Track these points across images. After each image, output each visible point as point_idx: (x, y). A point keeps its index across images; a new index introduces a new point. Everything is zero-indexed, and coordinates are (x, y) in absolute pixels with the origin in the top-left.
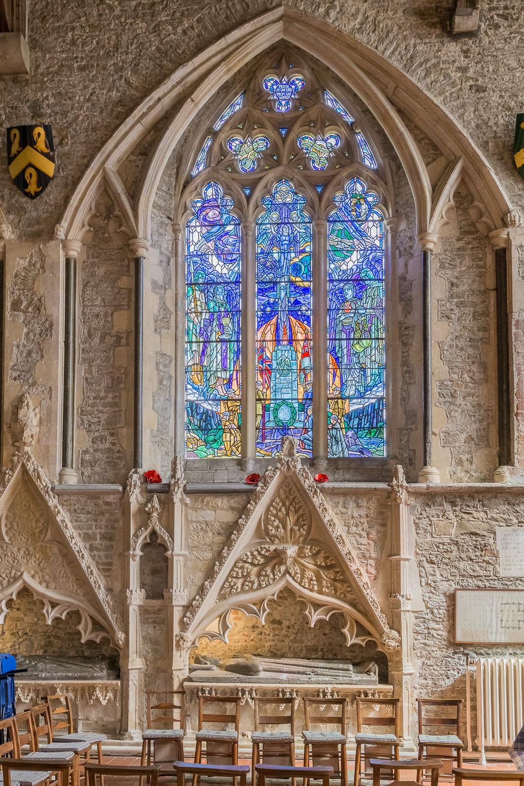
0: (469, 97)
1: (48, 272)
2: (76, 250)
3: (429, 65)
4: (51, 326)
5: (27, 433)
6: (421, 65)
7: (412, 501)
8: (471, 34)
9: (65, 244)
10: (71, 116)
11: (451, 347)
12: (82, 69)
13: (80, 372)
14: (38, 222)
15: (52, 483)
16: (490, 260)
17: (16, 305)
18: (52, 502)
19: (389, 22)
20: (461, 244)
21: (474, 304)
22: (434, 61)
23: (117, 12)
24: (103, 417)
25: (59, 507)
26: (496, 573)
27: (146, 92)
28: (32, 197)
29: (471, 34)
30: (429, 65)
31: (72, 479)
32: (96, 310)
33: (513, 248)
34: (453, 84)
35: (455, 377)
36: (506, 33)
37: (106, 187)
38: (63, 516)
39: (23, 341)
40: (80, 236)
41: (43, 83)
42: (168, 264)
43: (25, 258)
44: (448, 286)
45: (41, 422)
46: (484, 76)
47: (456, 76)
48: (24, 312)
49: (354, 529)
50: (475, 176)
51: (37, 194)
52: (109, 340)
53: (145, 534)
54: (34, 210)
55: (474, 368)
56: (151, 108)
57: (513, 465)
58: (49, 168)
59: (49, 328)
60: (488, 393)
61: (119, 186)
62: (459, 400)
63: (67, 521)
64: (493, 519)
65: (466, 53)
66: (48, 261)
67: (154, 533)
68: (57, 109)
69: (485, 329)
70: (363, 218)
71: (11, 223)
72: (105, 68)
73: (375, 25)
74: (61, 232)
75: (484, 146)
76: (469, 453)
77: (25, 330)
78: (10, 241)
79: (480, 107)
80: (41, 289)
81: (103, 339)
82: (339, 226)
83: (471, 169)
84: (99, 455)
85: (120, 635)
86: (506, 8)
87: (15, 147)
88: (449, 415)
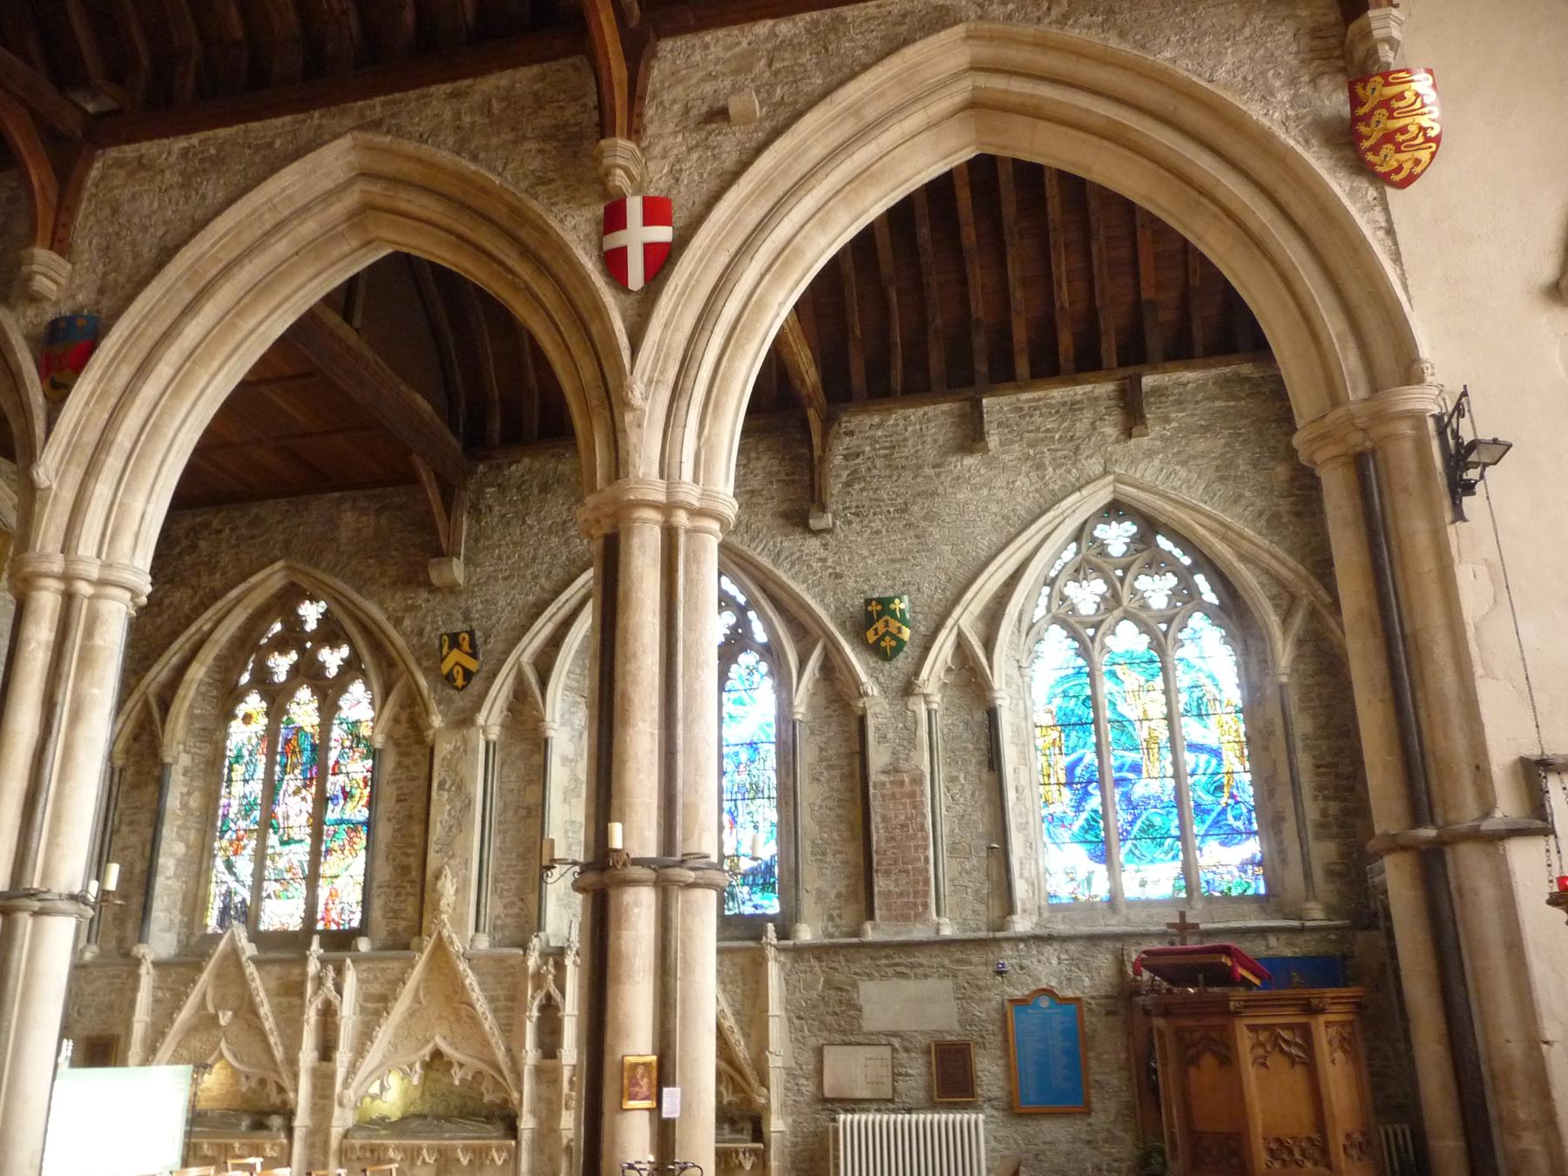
0: (828, 583)
1: (469, 756)
2: (495, 733)
3: (794, 557)
4: (470, 802)
5: (443, 903)
6: (787, 558)
7: (782, 959)
9: (485, 730)
10: (494, 618)
11: (821, 807)
12: (505, 579)
13: (496, 841)
14: (463, 712)
15: (464, 948)
16: (854, 726)
17: (441, 786)
18: (463, 966)
19: (759, 524)
20: (829, 712)
21: (841, 767)
22: (798, 554)
23: (536, 530)
24: (513, 885)
25: (469, 971)
26: (860, 1027)
27: (557, 593)
28: (456, 688)
30: (794, 557)
31: (483, 943)
32: (512, 786)
33: (869, 715)
34: (815, 573)
35: (825, 836)
36: (858, 528)
37: (520, 679)
38: (471, 980)
39: (446, 816)
40: (499, 721)
41: (473, 592)
42: (581, 738)
43: (450, 743)
44: (817, 750)
45: (457, 891)
46: (840, 564)
48: (448, 791)
49: (729, 987)
50: (834, 651)
51: (463, 687)
52: (523, 812)
53: (540, 996)
54: (460, 701)
55: (843, 827)
56: (559, 609)
58: (472, 665)
59: (469, 804)
60: (852, 851)
61: (532, 677)
62: (829, 858)
63: (475, 984)
64: (856, 973)
65: (825, 546)
66: (470, 745)
67: (549, 997)
68: (484, 613)
69: (851, 790)
71: (441, 713)
72: (524, 577)
73: (748, 527)
74: (481, 720)
75: (842, 626)
77: (448, 807)
78: (440, 729)
79: (839, 591)
80: (463, 770)
81: (516, 812)
82: (733, 695)
83: (830, 646)
84: (508, 920)
85: (515, 1095)
87: (445, 650)
88: (821, 874)
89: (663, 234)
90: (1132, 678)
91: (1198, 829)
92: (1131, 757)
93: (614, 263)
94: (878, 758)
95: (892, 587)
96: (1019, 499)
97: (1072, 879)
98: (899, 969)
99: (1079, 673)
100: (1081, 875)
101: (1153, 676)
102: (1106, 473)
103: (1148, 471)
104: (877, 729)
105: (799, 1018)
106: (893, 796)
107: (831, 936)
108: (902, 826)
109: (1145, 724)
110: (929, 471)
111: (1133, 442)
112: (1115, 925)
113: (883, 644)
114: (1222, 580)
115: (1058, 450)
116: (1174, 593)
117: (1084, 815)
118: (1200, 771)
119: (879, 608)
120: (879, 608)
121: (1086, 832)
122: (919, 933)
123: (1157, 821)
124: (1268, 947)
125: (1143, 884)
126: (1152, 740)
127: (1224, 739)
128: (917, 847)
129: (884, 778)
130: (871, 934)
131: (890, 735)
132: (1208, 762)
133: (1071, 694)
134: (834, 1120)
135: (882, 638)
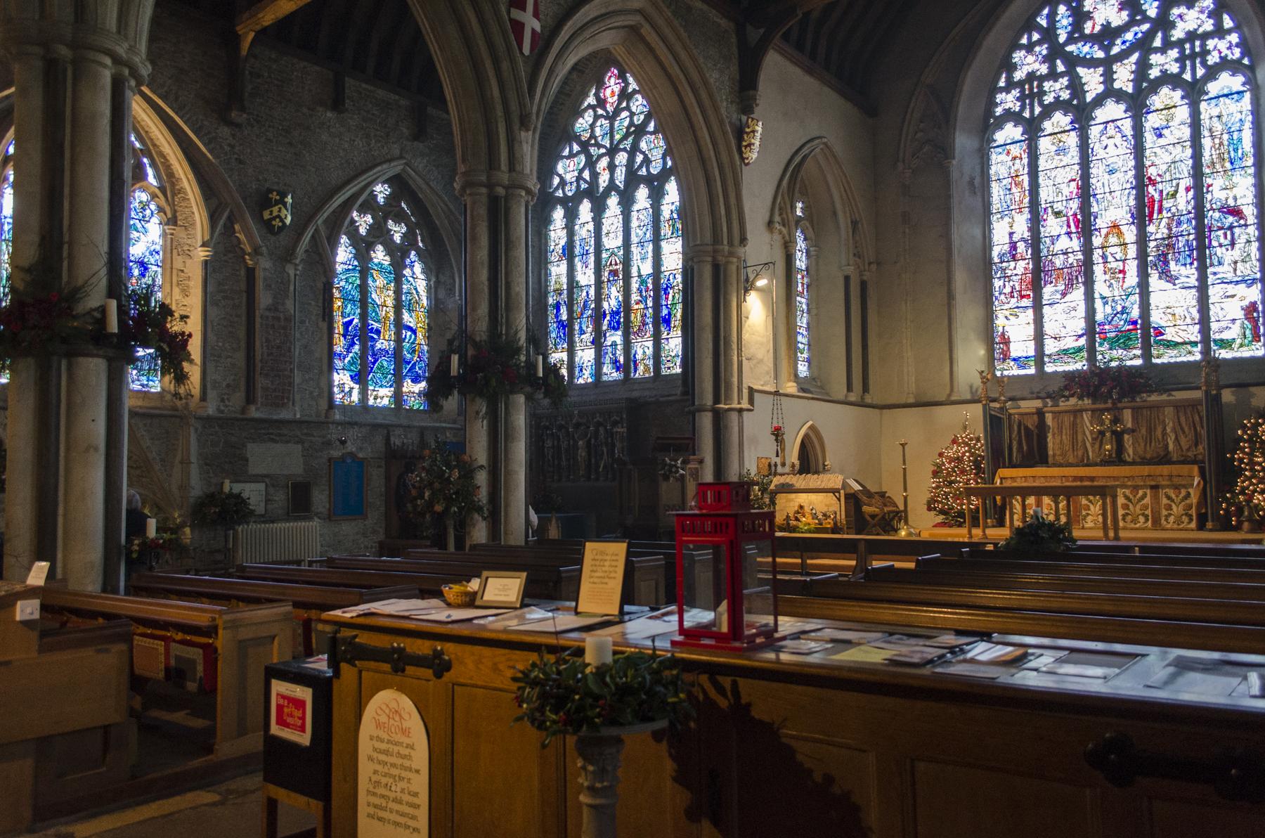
8: (238, 126)
16: (243, 272)
29: (238, 126)
35: (220, 344)
47: (227, 148)
57: (257, 404)
64: (245, 438)
65: (233, 136)
70: (147, 219)
76: (228, 394)
86: (257, 115)
89: (537, 26)
90: (380, 281)
91: (405, 371)
92: (376, 325)
93: (518, 27)
94: (264, 299)
95: (278, 183)
96: (356, 153)
97: (343, 391)
98: (272, 436)
99: (355, 269)
100: (347, 390)
101: (391, 282)
102: (401, 157)
103: (420, 163)
104: (265, 279)
105: (206, 464)
106: (273, 325)
107: (222, 412)
108: (278, 347)
109: (385, 308)
110: (305, 110)
111: (416, 143)
112: (368, 419)
113: (274, 223)
114: (434, 237)
115: (377, 130)
116: (404, 236)
117: (351, 355)
118: (407, 341)
119: (278, 198)
120: (278, 198)
121: (352, 365)
122: (284, 415)
123: (385, 364)
124: (446, 437)
125: (376, 398)
126: (386, 318)
127: (419, 325)
128: (286, 362)
129: (267, 313)
130: (254, 412)
131: (273, 286)
132: (411, 336)
133: (350, 281)
134: (234, 529)
135: (274, 219)
